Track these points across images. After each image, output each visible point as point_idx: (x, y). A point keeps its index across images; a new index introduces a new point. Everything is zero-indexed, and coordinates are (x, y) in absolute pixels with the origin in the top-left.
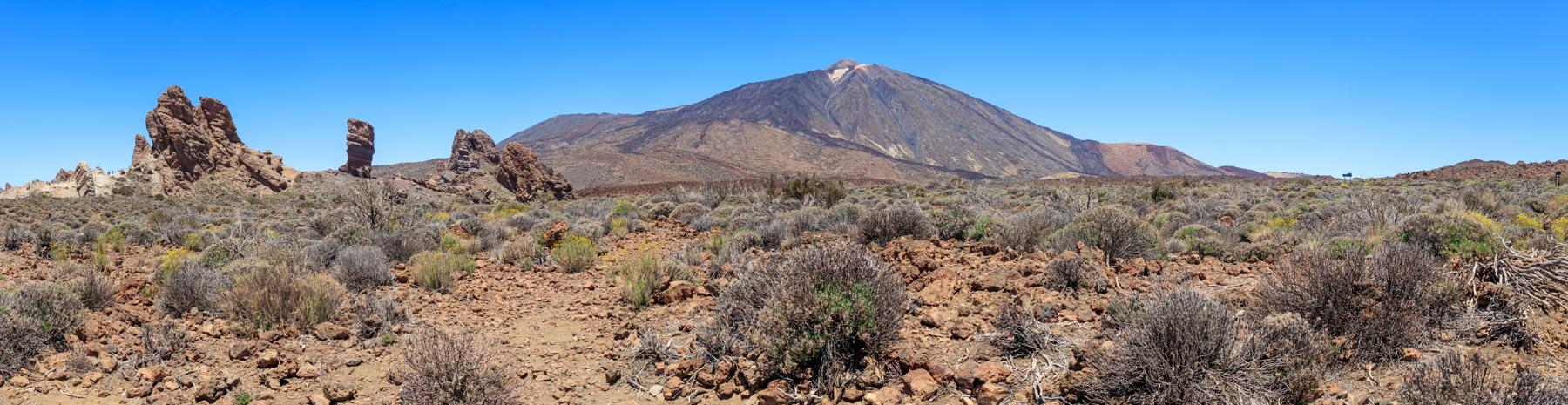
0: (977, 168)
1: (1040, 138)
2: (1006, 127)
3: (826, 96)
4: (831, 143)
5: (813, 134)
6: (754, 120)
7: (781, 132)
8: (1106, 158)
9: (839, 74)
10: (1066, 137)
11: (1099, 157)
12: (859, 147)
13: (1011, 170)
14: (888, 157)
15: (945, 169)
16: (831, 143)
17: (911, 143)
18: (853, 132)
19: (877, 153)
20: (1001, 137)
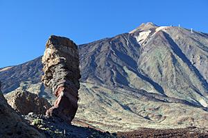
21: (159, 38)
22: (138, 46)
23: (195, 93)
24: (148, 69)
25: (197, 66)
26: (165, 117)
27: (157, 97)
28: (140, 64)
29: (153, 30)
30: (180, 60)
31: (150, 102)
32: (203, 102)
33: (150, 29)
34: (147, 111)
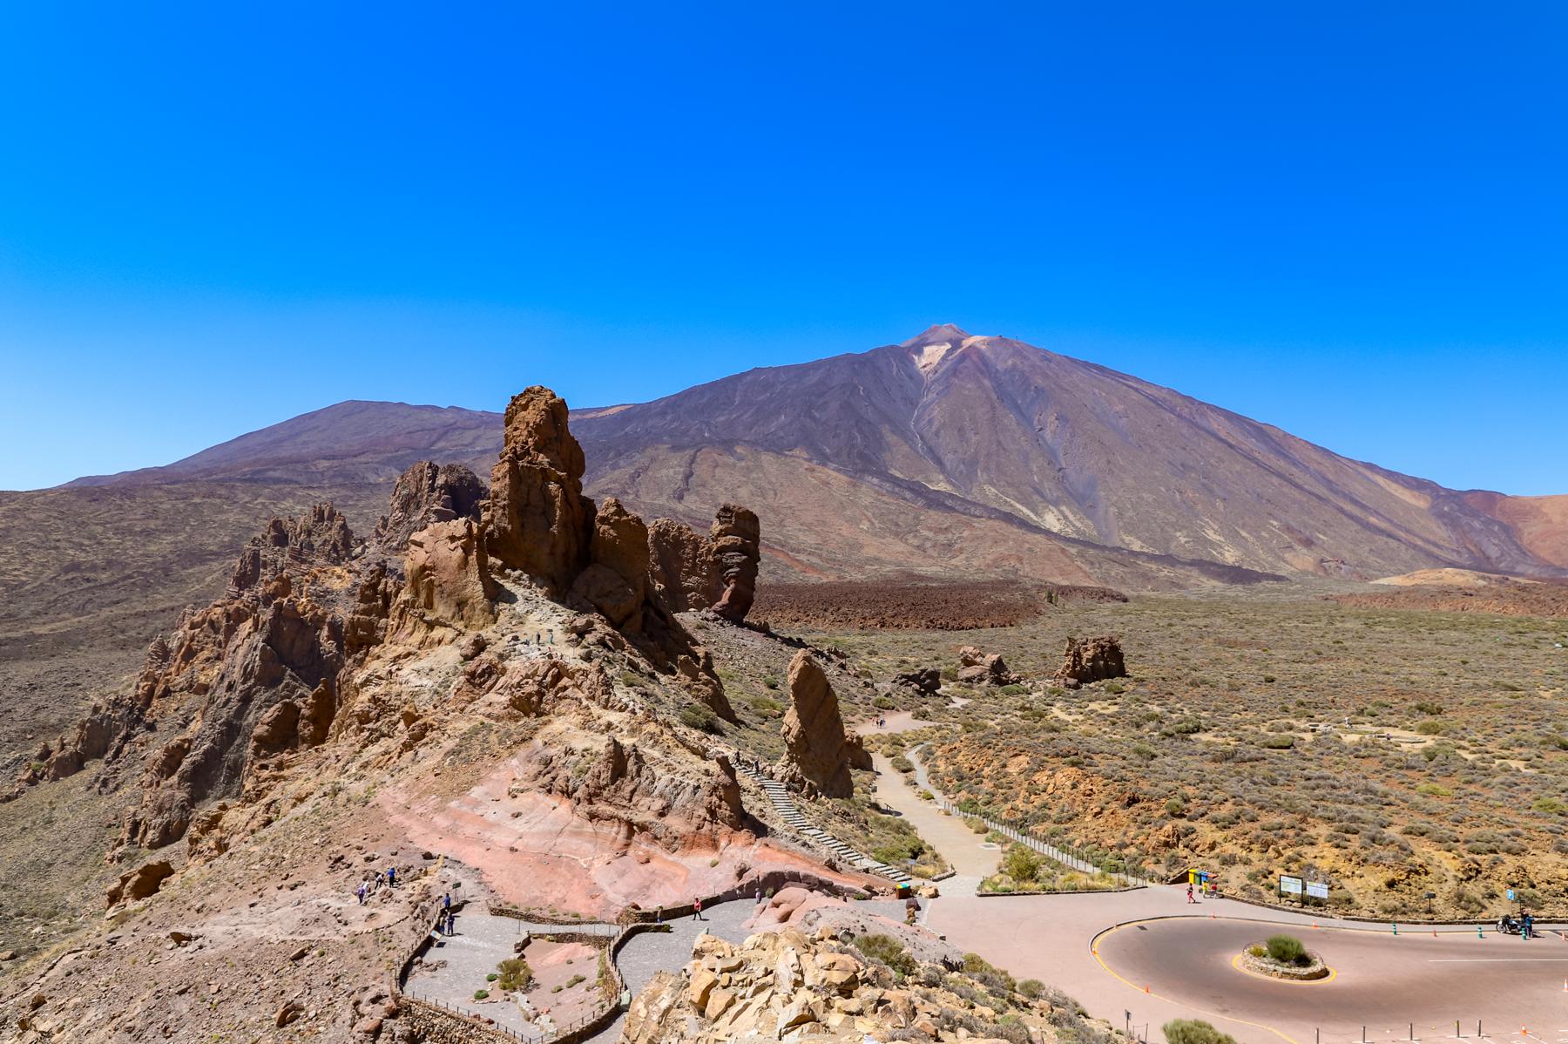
0: (1230, 556)
1: (1359, 489)
2: (1280, 464)
3: (912, 403)
4: (936, 501)
5: (896, 481)
6: (777, 447)
7: (837, 478)
9: (932, 355)
10: (1418, 485)
11: (1509, 532)
15: (1169, 560)
16: (936, 501)
19: (1024, 524)
21: (968, 363)
22: (914, 377)
23: (1036, 497)
24: (937, 434)
25: (1048, 434)
26: (961, 550)
27: (949, 503)
28: (917, 422)
29: (956, 344)
30: (1010, 420)
31: (931, 512)
32: (1051, 521)
33: (950, 341)
34: (926, 533)
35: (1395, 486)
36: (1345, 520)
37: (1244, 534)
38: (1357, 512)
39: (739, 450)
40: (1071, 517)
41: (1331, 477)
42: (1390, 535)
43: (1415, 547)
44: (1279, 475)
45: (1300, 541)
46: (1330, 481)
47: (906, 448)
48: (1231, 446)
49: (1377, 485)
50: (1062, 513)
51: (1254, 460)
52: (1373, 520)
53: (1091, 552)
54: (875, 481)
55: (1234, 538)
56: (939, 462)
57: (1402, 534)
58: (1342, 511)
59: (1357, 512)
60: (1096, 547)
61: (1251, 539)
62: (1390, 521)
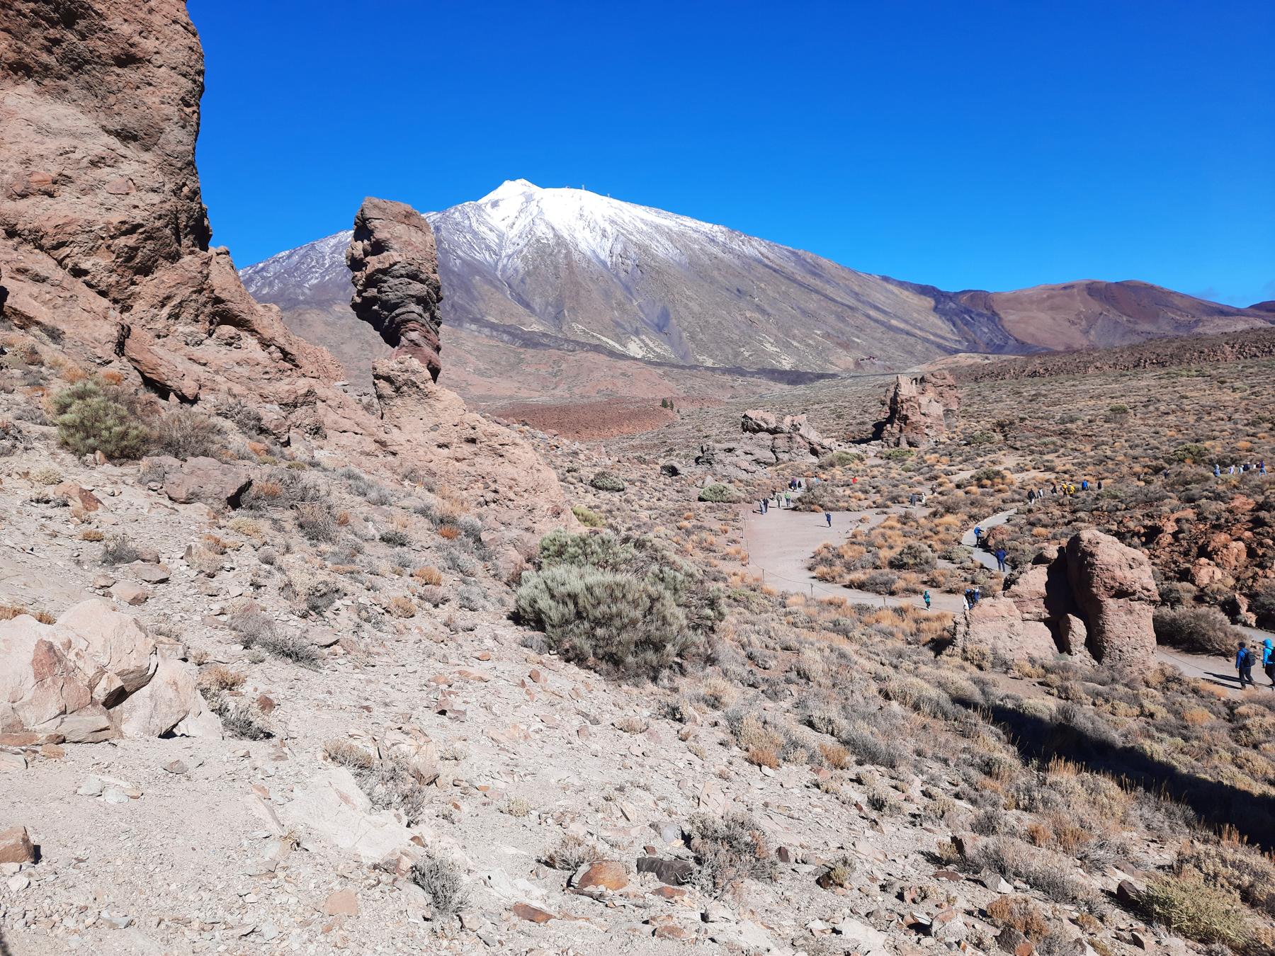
0: (787, 363)
4: (530, 341)
5: (493, 327)
8: (1010, 318)
10: (924, 290)
12: (582, 345)
13: (842, 361)
14: (635, 359)
15: (739, 371)
17: (661, 327)
18: (558, 317)
19: (612, 354)
20: (812, 303)
23: (618, 330)
24: (523, 281)
27: (545, 341)
31: (531, 351)
32: (634, 349)
35: (906, 293)
36: (872, 323)
37: (795, 344)
38: (880, 317)
39: (337, 308)
40: (651, 345)
41: (857, 289)
42: (908, 333)
43: (928, 340)
44: (817, 292)
45: (840, 345)
46: (857, 294)
47: (498, 295)
48: (775, 271)
49: (893, 293)
50: (643, 341)
51: (795, 281)
52: (894, 322)
53: (675, 370)
54: (474, 327)
55: (787, 346)
56: (527, 306)
57: (918, 332)
58: (869, 317)
59: (880, 317)
60: (677, 366)
61: (802, 347)
62: (906, 322)
